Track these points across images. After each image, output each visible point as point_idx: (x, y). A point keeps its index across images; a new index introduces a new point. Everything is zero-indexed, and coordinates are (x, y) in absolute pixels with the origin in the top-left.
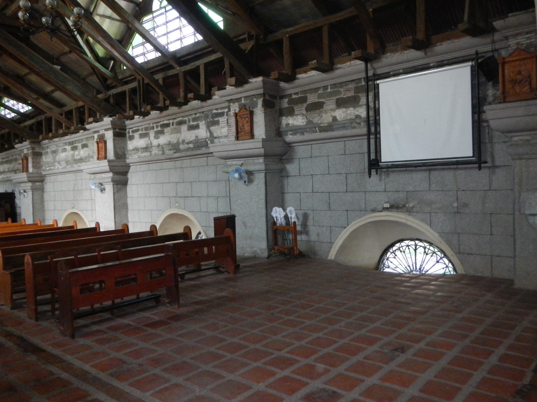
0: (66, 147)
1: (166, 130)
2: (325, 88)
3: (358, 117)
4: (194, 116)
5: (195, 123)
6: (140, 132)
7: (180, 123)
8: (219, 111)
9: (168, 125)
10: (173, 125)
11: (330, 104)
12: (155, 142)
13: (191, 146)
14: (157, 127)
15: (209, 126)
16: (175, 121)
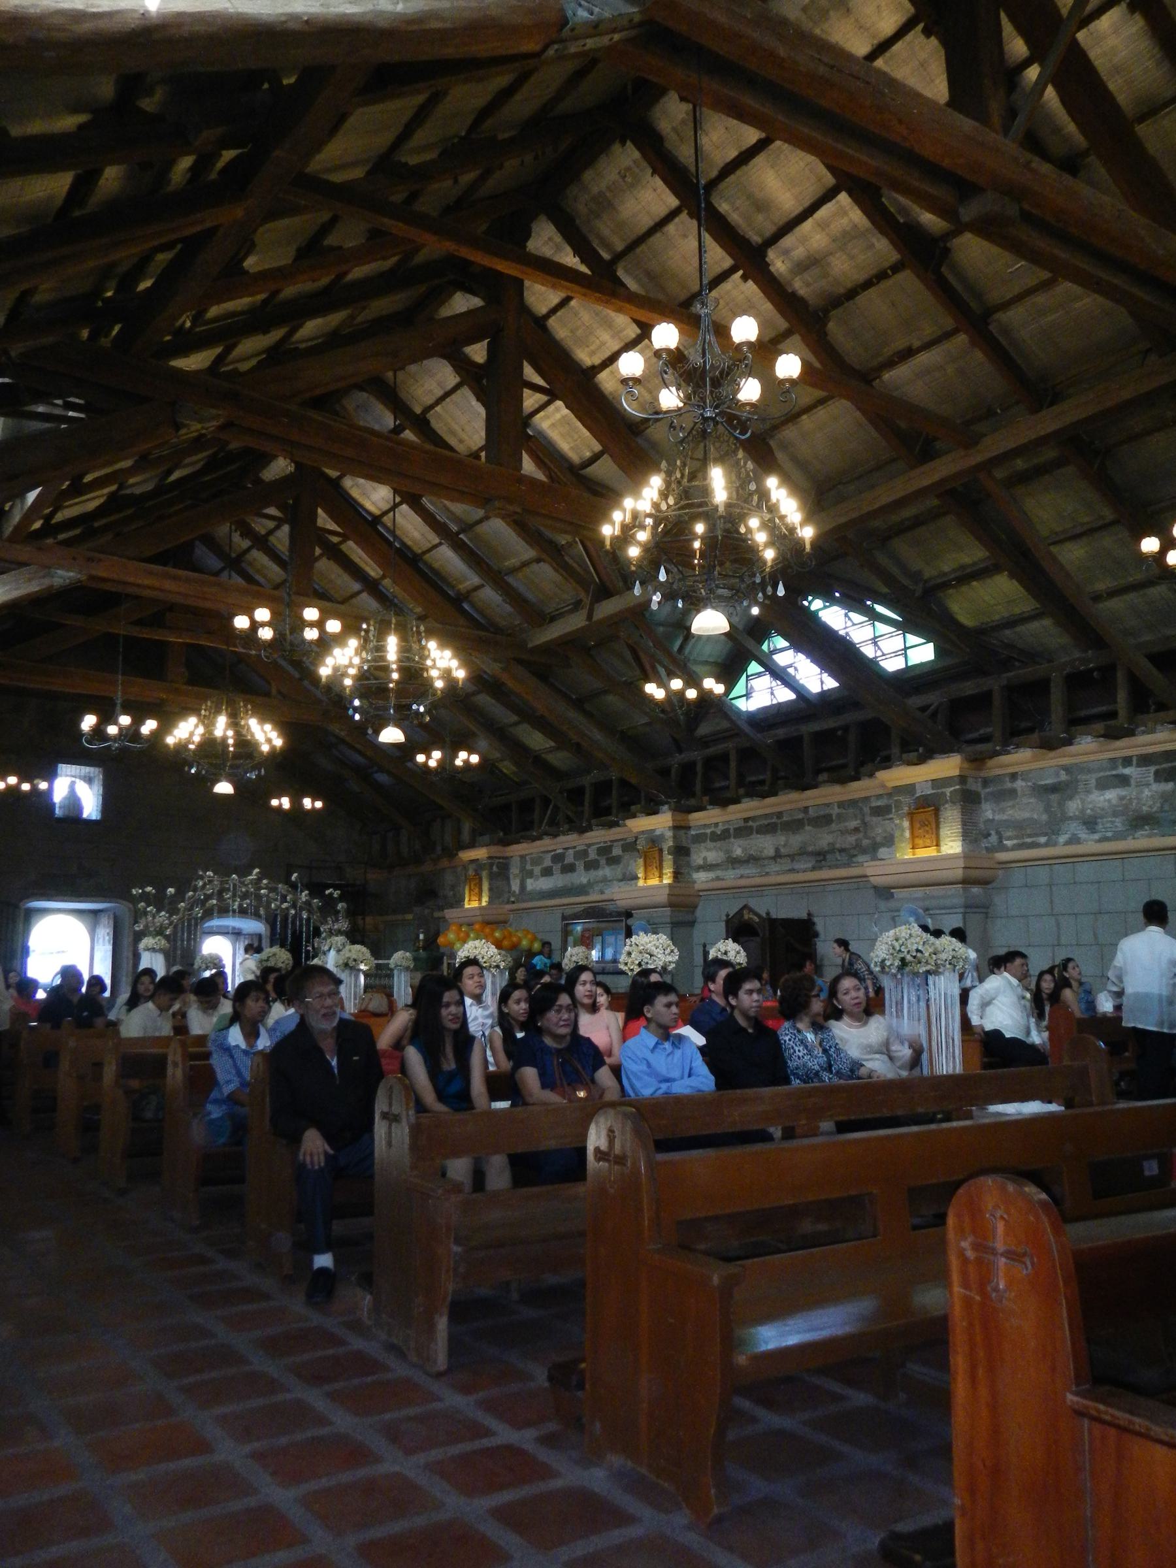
0: (1127, 771)
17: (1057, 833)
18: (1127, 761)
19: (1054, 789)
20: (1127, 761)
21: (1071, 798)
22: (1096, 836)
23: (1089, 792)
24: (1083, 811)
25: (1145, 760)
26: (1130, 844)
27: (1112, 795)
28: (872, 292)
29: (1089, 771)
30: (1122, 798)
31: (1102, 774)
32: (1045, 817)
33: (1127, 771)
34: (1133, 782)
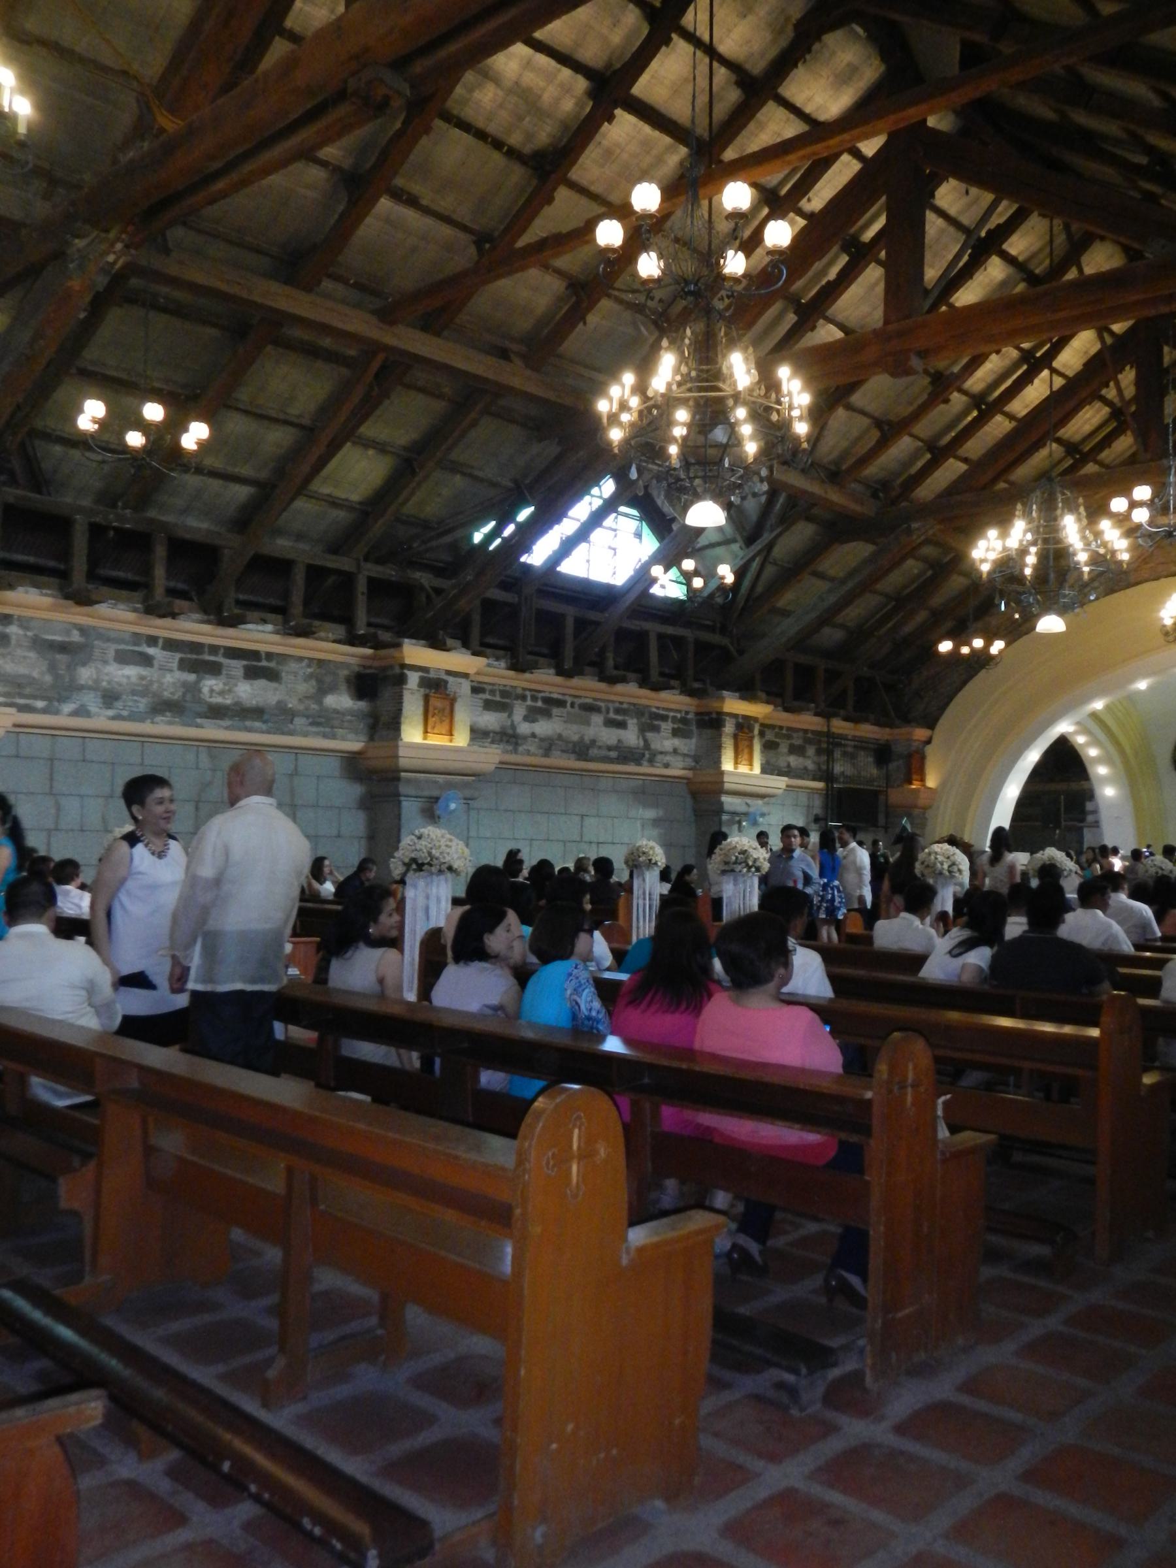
0: (151, 651)
1: (555, 711)
2: (781, 728)
3: (805, 768)
4: (617, 705)
5: (619, 718)
6: (487, 696)
7: (590, 708)
8: (661, 712)
9: (560, 703)
10: (572, 705)
11: (784, 748)
12: (524, 728)
13: (613, 754)
14: (534, 699)
15: (643, 729)
16: (578, 701)
17: (62, 699)
18: (152, 641)
19: (63, 648)
20: (152, 641)
21: (84, 664)
22: (110, 713)
23: (105, 662)
24: (97, 681)
25: (171, 645)
26: (146, 727)
27: (131, 672)
28: (467, 139)
29: (108, 640)
30: (142, 678)
31: (122, 647)
32: (48, 678)
33: (151, 651)
34: (156, 663)
